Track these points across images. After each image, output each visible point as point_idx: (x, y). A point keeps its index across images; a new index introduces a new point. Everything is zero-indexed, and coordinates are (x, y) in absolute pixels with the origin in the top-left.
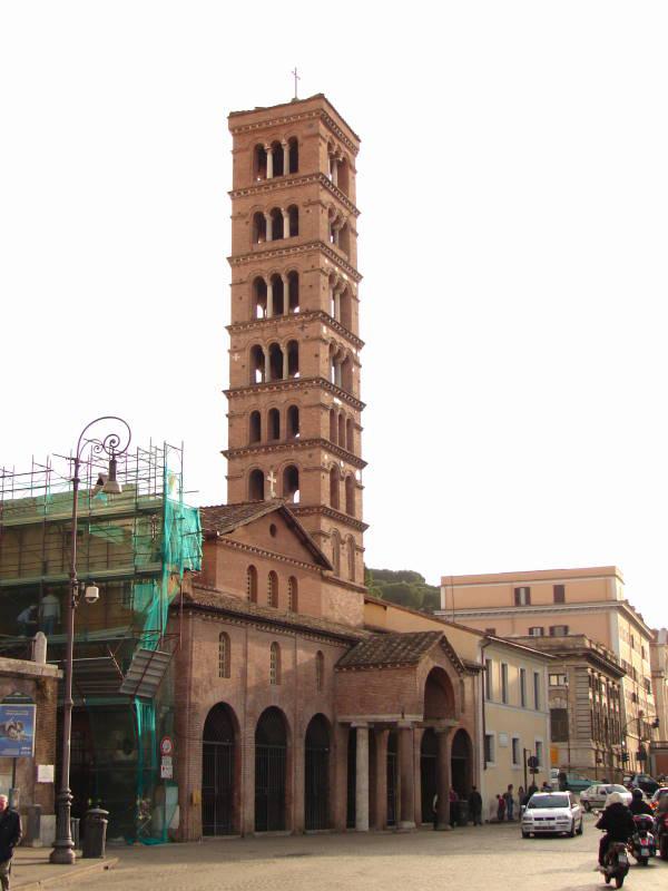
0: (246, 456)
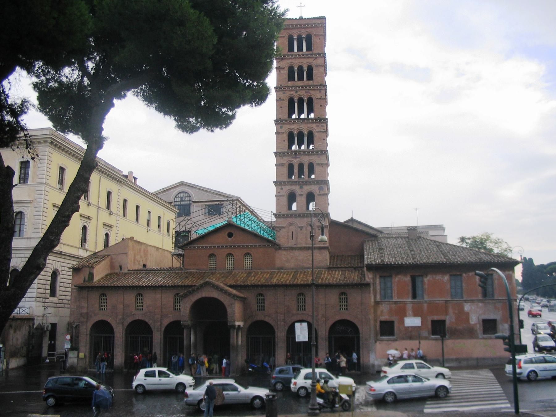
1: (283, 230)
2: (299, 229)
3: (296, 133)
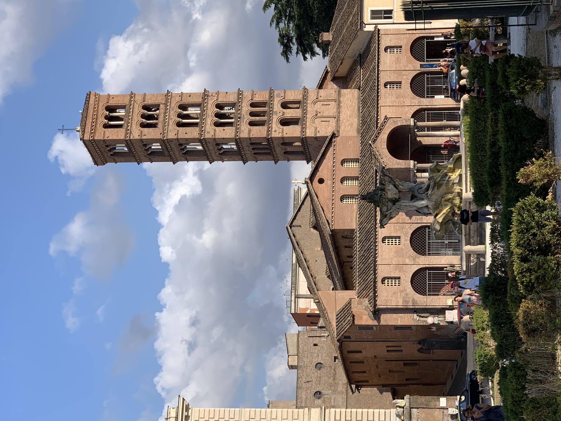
0: (277, 156)
1: (318, 129)
2: (319, 115)
3: (216, 119)
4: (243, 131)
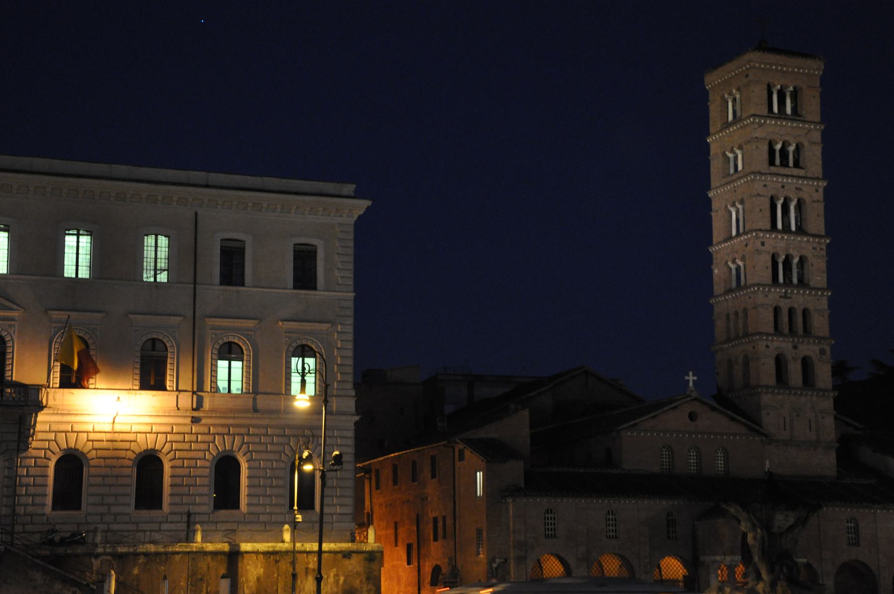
4: (766, 296)
